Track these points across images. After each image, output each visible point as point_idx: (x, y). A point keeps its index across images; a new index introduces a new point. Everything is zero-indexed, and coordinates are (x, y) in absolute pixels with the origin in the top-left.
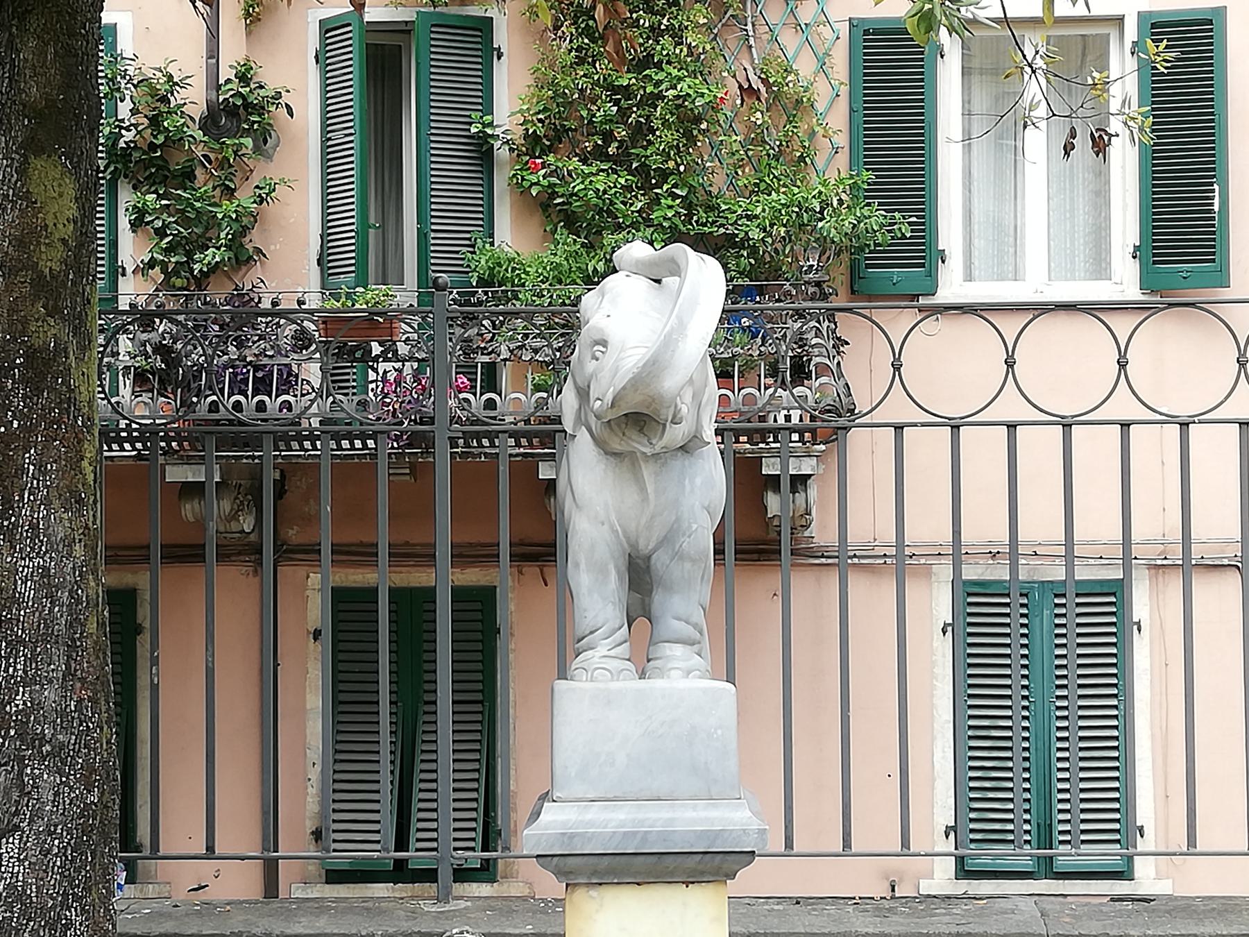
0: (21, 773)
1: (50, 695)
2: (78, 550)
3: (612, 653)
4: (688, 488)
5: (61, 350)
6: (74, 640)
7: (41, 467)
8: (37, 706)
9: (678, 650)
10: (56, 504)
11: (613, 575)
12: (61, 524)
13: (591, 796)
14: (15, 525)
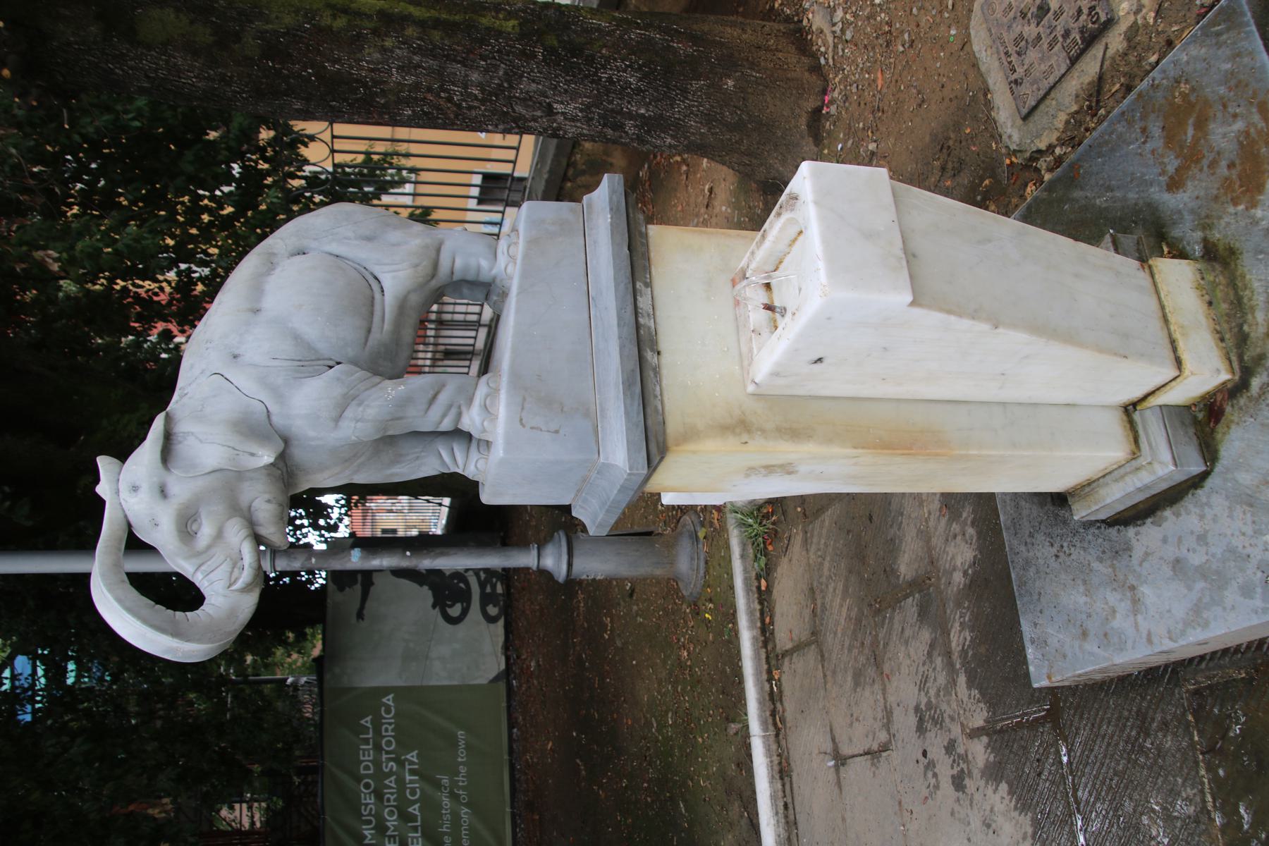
1: (475, 76)
2: (388, 43)
7: (338, 61)
8: (480, 85)
10: (359, 55)
12: (371, 55)
14: (372, 79)
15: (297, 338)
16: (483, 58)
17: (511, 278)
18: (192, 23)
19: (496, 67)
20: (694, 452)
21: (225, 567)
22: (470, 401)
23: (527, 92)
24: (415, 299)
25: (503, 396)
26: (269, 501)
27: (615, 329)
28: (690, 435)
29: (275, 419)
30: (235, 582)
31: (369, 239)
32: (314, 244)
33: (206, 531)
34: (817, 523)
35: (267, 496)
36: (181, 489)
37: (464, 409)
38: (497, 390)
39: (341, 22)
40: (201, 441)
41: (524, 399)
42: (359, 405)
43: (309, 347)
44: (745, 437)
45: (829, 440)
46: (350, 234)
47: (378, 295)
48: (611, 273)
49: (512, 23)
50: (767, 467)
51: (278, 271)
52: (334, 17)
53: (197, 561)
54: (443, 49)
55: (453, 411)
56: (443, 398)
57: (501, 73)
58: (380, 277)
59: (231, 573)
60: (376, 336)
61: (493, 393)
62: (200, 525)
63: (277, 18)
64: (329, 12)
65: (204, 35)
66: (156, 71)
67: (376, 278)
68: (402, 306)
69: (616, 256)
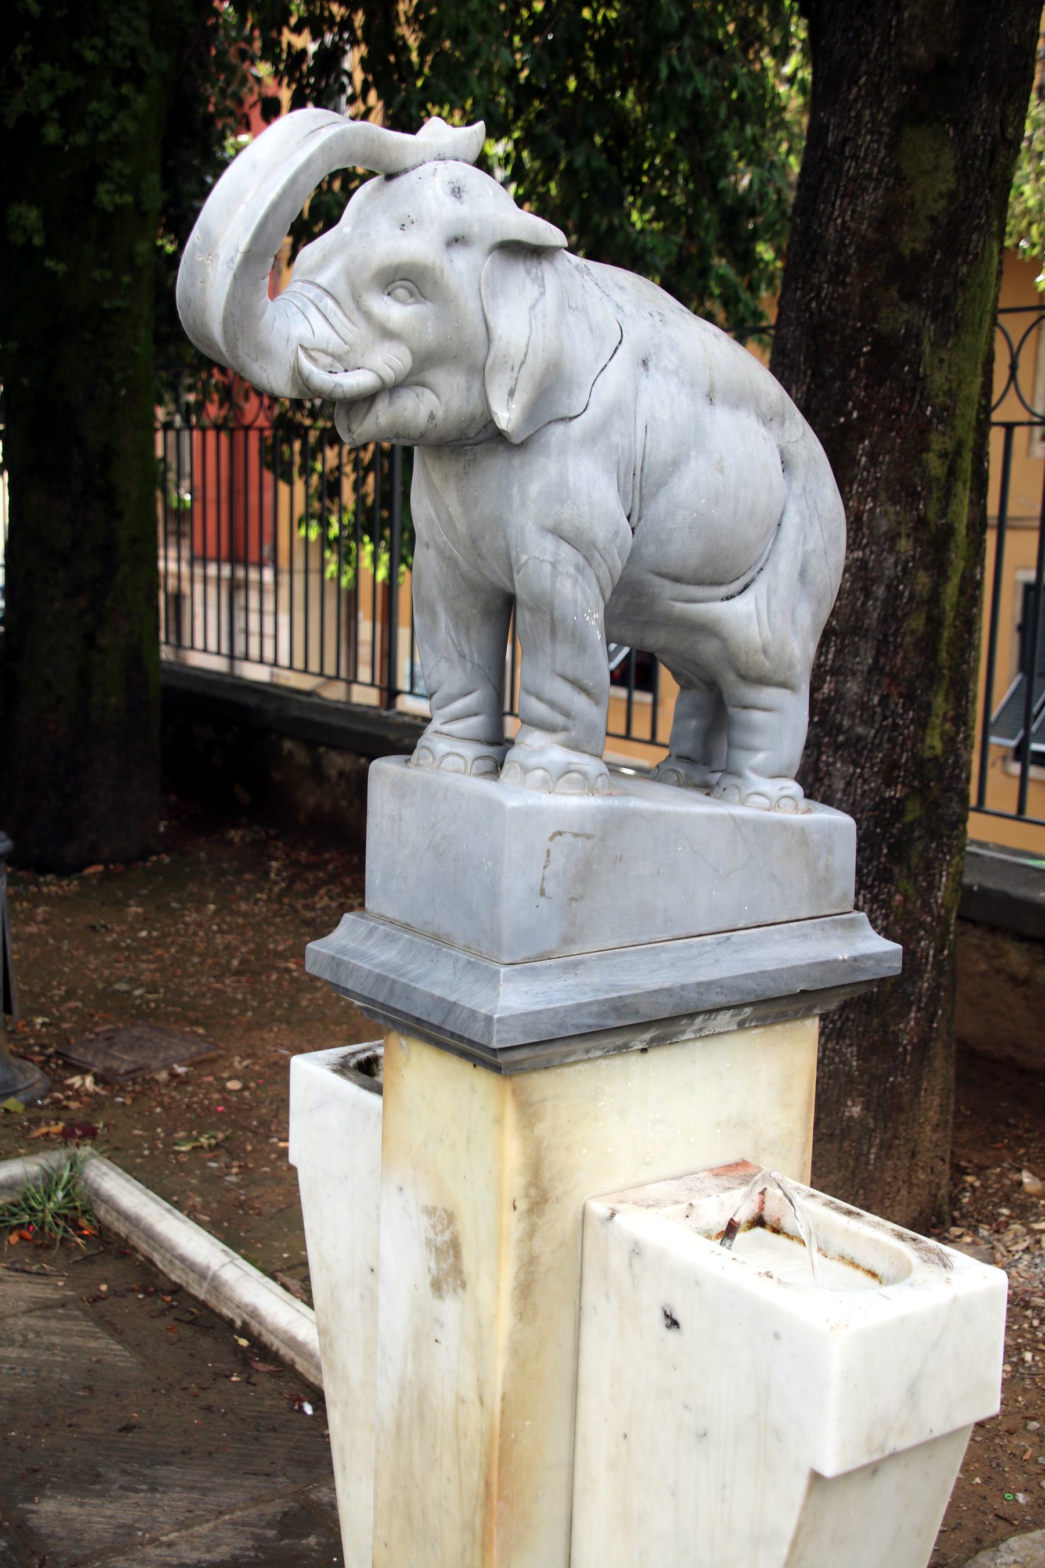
0: (818, 758)
1: (853, 687)
2: (904, 545)
3: (446, 728)
4: (516, 502)
5: (914, 336)
6: (886, 636)
7: (873, 461)
9: (536, 739)
10: (883, 496)
11: (444, 620)
13: (389, 915)
15: (675, 465)
16: (884, 700)
17: (743, 802)
18: (932, 219)
19: (869, 722)
20: (499, 1121)
21: (334, 343)
22: (574, 746)
23: (828, 774)
24: (709, 648)
25: (593, 802)
26: (432, 417)
27: (692, 979)
28: (528, 1112)
29: (558, 429)
30: (311, 357)
31: (803, 573)
32: (797, 486)
33: (395, 311)
34: (87, 1326)
35: (440, 414)
36: (462, 270)
37: (561, 736)
38: (592, 791)
39: (935, 466)
40: (532, 307)
41: (589, 837)
42: (577, 568)
43: (660, 485)
44: (522, 1205)
45: (515, 1350)
46: (810, 546)
47: (723, 591)
48: (770, 966)
49: (938, 745)
50: (454, 1246)
51: (763, 430)
52: (943, 455)
53: (342, 290)
54: (895, 634)
55: (559, 719)
56: (580, 703)
57: (860, 730)
58: (749, 595)
59: (325, 352)
60: (669, 589)
61: (588, 786)
62: (398, 300)
63: (941, 361)
64: (950, 446)
65: (912, 240)
66: (855, 157)
67: (746, 587)
68: (705, 629)
69: (793, 971)
